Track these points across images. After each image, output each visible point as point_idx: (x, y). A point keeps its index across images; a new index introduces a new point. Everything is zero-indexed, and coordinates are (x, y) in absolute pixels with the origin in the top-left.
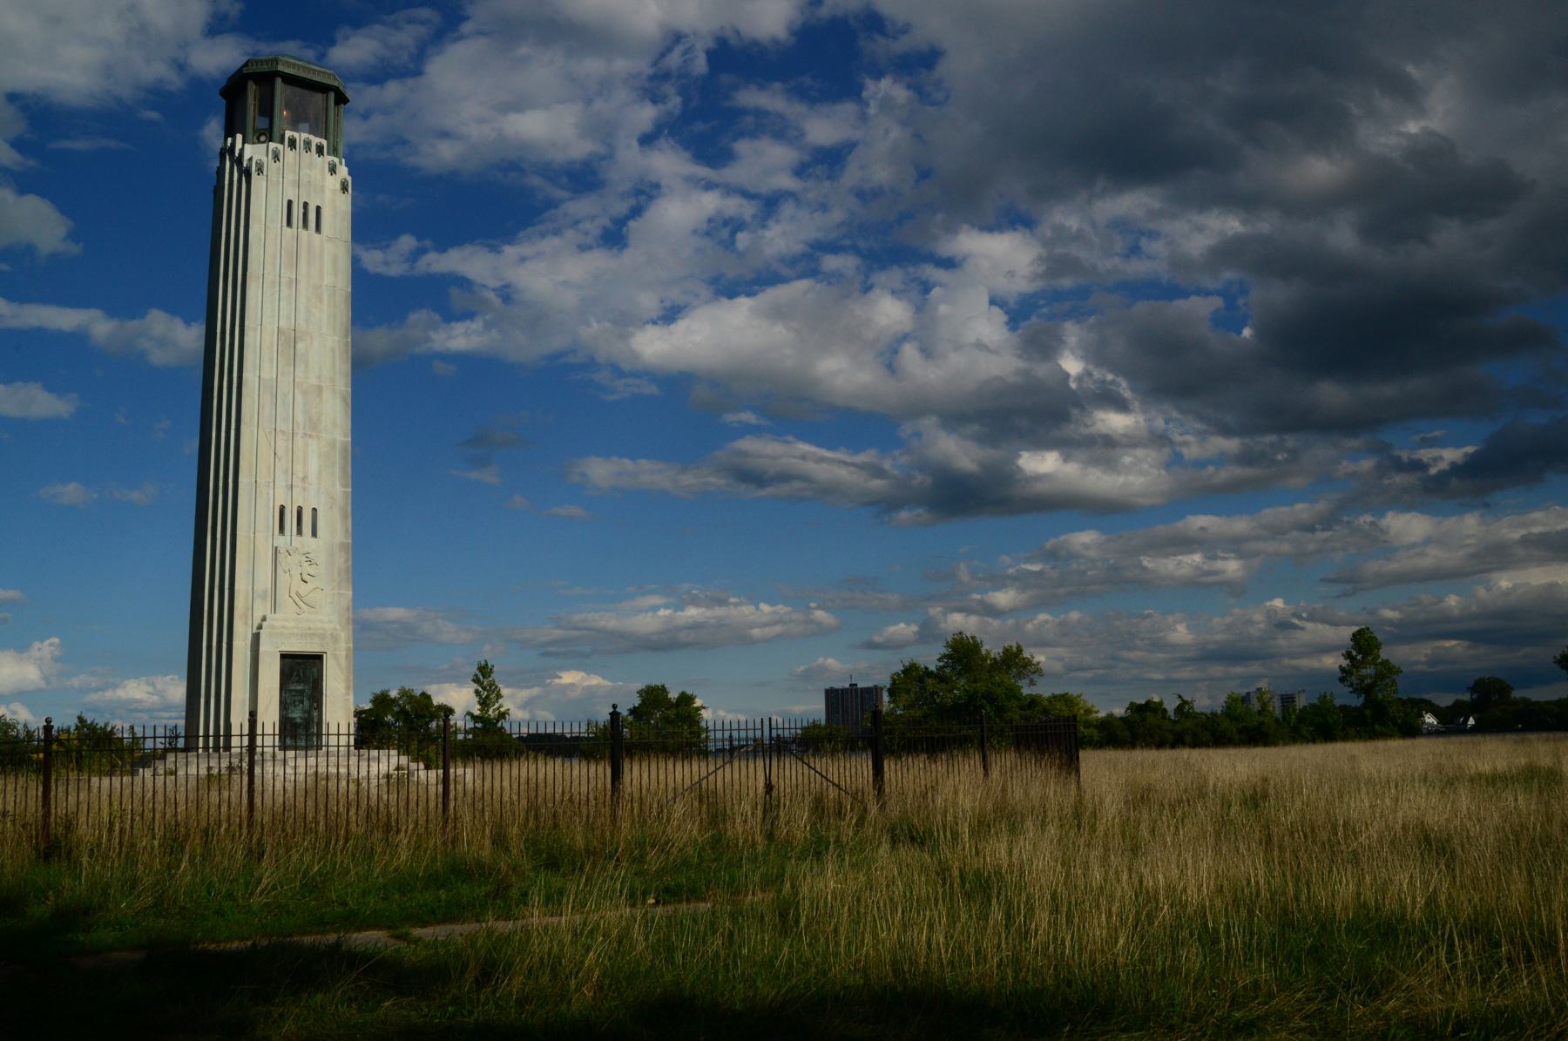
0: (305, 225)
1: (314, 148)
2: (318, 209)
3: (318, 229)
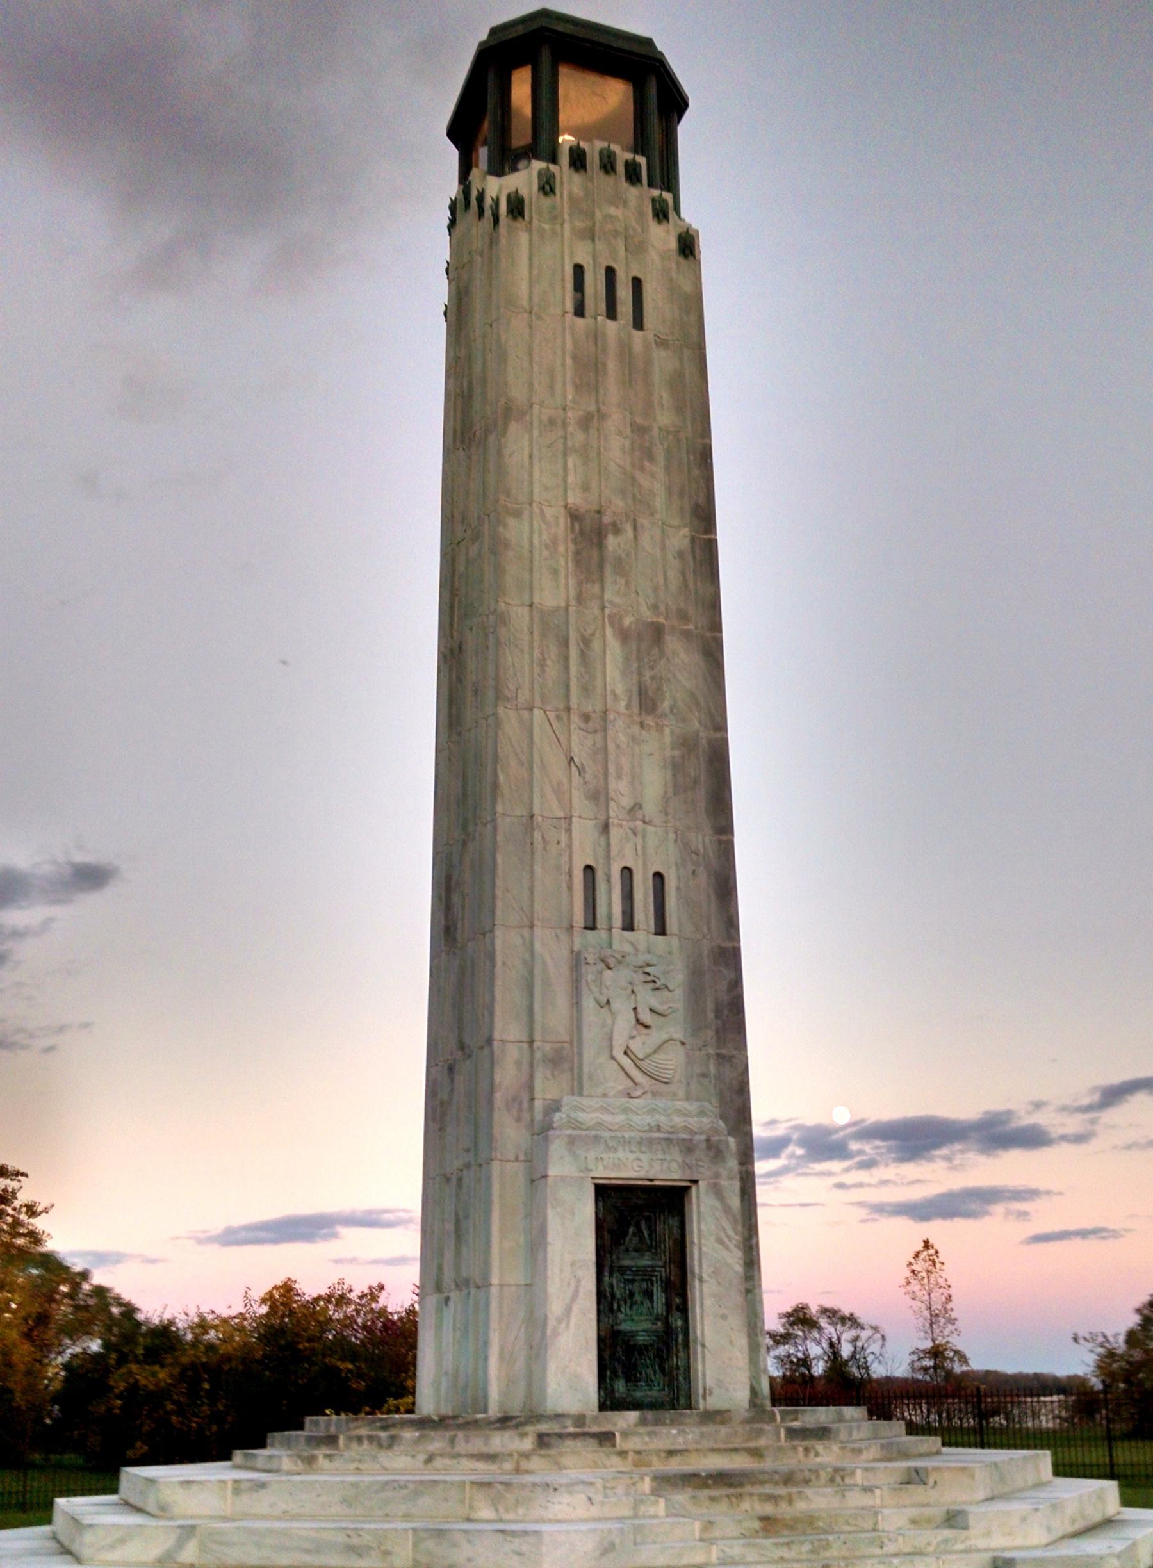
0: (612, 313)
1: (620, 168)
2: (637, 283)
3: (638, 323)
